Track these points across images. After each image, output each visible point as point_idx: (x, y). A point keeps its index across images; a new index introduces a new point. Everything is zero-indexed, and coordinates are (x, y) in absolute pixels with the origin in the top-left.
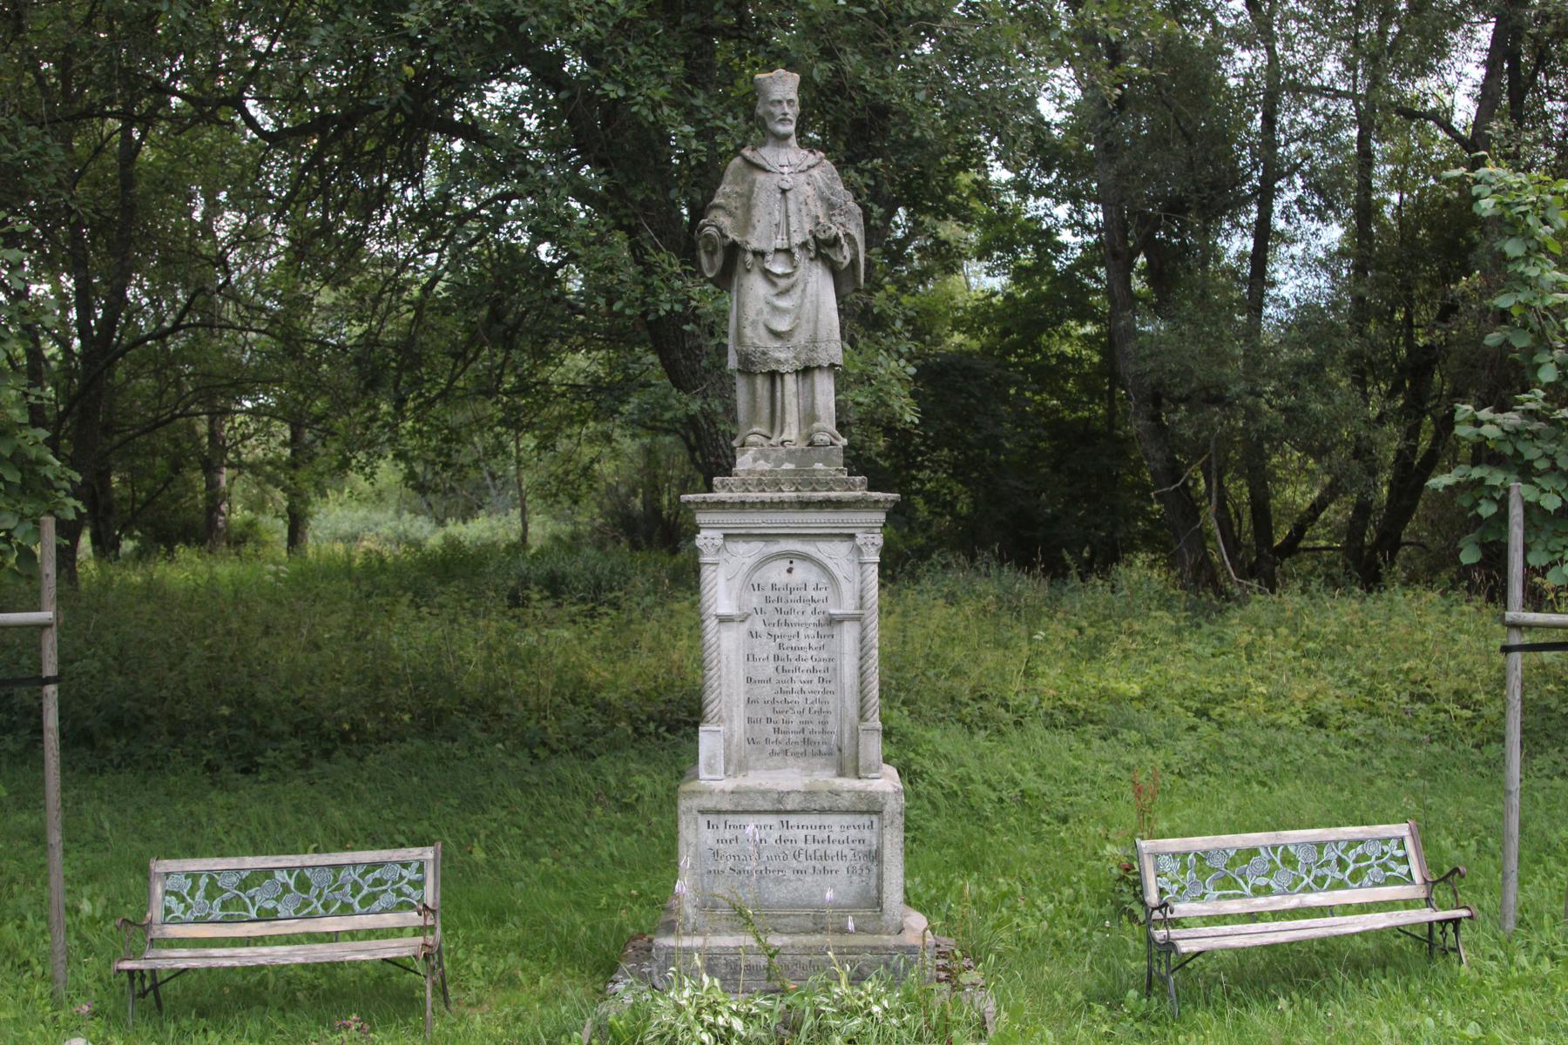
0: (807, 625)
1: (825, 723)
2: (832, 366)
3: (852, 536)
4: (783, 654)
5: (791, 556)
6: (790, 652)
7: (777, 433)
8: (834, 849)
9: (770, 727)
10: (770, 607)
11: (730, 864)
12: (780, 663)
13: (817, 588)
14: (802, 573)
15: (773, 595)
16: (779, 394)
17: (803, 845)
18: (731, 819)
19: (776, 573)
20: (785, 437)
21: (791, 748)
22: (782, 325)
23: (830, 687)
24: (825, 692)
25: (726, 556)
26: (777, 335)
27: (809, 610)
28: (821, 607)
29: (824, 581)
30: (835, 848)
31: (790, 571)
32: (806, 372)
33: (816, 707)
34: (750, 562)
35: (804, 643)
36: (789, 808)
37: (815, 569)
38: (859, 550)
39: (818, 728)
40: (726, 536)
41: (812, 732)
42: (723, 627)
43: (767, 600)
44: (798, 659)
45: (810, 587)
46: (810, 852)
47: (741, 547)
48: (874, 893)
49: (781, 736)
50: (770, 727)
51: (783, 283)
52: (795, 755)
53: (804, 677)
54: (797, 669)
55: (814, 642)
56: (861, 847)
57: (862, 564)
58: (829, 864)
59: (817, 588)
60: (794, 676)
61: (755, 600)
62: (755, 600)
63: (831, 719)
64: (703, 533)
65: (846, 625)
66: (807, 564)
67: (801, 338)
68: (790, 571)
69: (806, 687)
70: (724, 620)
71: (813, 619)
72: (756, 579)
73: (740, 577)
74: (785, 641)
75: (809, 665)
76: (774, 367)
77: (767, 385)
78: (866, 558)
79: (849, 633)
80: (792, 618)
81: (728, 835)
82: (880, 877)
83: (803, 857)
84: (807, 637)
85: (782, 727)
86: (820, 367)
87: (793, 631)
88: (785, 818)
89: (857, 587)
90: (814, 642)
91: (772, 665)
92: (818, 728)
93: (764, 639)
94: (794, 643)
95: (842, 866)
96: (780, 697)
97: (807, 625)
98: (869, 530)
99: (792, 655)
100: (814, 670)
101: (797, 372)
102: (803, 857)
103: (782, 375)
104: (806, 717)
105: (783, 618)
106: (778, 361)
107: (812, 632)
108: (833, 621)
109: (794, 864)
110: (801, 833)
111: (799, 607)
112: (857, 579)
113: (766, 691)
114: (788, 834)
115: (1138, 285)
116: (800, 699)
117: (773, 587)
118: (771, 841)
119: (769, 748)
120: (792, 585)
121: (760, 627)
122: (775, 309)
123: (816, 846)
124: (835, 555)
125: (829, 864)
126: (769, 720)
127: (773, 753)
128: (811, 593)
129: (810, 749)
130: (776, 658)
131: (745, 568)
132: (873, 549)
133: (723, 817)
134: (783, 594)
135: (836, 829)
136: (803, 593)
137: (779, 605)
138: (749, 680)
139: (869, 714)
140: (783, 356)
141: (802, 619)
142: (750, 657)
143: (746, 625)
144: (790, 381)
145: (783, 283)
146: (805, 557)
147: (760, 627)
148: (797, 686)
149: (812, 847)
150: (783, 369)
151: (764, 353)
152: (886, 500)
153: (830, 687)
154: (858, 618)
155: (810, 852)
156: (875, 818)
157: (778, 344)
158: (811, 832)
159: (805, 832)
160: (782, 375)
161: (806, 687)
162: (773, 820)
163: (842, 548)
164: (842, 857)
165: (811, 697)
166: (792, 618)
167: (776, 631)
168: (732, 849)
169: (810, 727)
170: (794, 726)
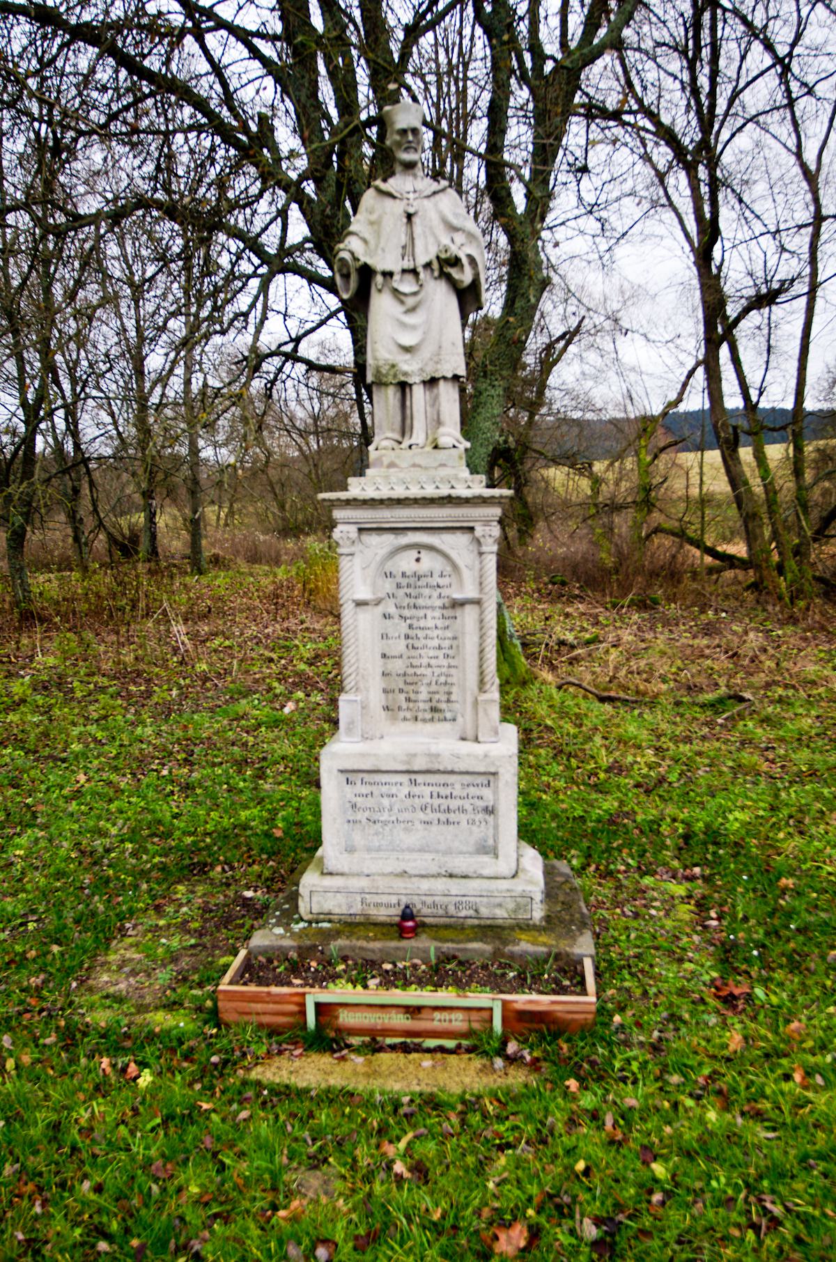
0: (433, 608)
1: (449, 693)
2: (456, 378)
3: (472, 529)
4: (412, 633)
5: (419, 547)
7: (407, 437)
8: (454, 804)
9: (402, 697)
10: (401, 592)
11: (367, 814)
12: (410, 641)
14: (429, 562)
15: (404, 582)
16: (408, 403)
17: (429, 800)
18: (367, 777)
19: (406, 562)
20: (413, 441)
21: (420, 715)
22: (408, 340)
23: (453, 662)
24: (449, 667)
25: (360, 547)
26: (407, 349)
27: (435, 594)
28: (445, 592)
29: (449, 569)
30: (454, 804)
31: (418, 560)
32: (432, 382)
33: (442, 679)
34: (383, 552)
35: (430, 623)
36: (416, 768)
37: (440, 559)
38: (479, 543)
39: (444, 698)
40: (360, 530)
41: (438, 701)
42: (359, 609)
43: (399, 586)
45: (436, 575)
46: (435, 806)
47: (373, 539)
48: (491, 842)
49: (411, 705)
50: (402, 697)
51: (410, 301)
52: (424, 720)
53: (432, 653)
54: (425, 647)
55: (439, 625)
56: (481, 804)
57: (481, 554)
58: (452, 817)
60: (422, 652)
61: (389, 586)
62: (389, 586)
63: (454, 689)
64: (340, 528)
65: (468, 608)
66: (434, 554)
67: (426, 353)
68: (418, 560)
69: (433, 662)
70: (360, 604)
71: (439, 603)
72: (389, 567)
73: (373, 566)
74: (416, 624)
75: (436, 643)
76: (403, 379)
77: (399, 395)
78: (484, 549)
79: (469, 616)
80: (420, 602)
81: (365, 790)
82: (496, 827)
83: (429, 810)
84: (433, 619)
85: (413, 696)
86: (444, 378)
87: (421, 613)
88: (413, 777)
89: (477, 574)
90: (440, 623)
91: (403, 642)
92: (444, 698)
93: (397, 620)
94: (422, 623)
95: (463, 818)
97: (433, 608)
98: (487, 523)
99: (421, 634)
100: (440, 648)
101: (424, 382)
102: (429, 810)
103: (411, 385)
104: (434, 688)
105: (412, 601)
106: (405, 374)
107: (438, 613)
108: (457, 604)
109: (422, 816)
110: (427, 791)
111: (426, 592)
112: (477, 566)
113: (398, 666)
114: (416, 790)
116: (428, 671)
117: (404, 575)
118: (402, 795)
119: (402, 714)
120: (421, 573)
121: (392, 610)
122: (403, 325)
123: (441, 801)
124: (456, 544)
125: (452, 817)
126: (401, 691)
127: (405, 719)
128: (436, 580)
129: (436, 715)
130: (407, 637)
131: (378, 558)
132: (491, 541)
133: (361, 775)
134: (412, 580)
135: (458, 786)
136: (429, 580)
137: (408, 591)
138: (384, 656)
139: (488, 686)
140: (412, 368)
141: (429, 603)
142: (384, 636)
143: (380, 609)
144: (419, 393)
145: (410, 301)
146: (431, 548)
147: (392, 610)
148: (425, 661)
149: (436, 802)
150: (410, 381)
151: (393, 366)
152: (501, 497)
153: (453, 662)
154: (478, 602)
155: (435, 806)
156: (491, 778)
157: (408, 356)
158: (435, 789)
159: (431, 788)
160: (411, 385)
161: (433, 662)
162: (404, 778)
163: (463, 539)
164: (462, 810)
165: (437, 671)
167: (406, 613)
168: (370, 802)
169: (437, 697)
170: (424, 695)
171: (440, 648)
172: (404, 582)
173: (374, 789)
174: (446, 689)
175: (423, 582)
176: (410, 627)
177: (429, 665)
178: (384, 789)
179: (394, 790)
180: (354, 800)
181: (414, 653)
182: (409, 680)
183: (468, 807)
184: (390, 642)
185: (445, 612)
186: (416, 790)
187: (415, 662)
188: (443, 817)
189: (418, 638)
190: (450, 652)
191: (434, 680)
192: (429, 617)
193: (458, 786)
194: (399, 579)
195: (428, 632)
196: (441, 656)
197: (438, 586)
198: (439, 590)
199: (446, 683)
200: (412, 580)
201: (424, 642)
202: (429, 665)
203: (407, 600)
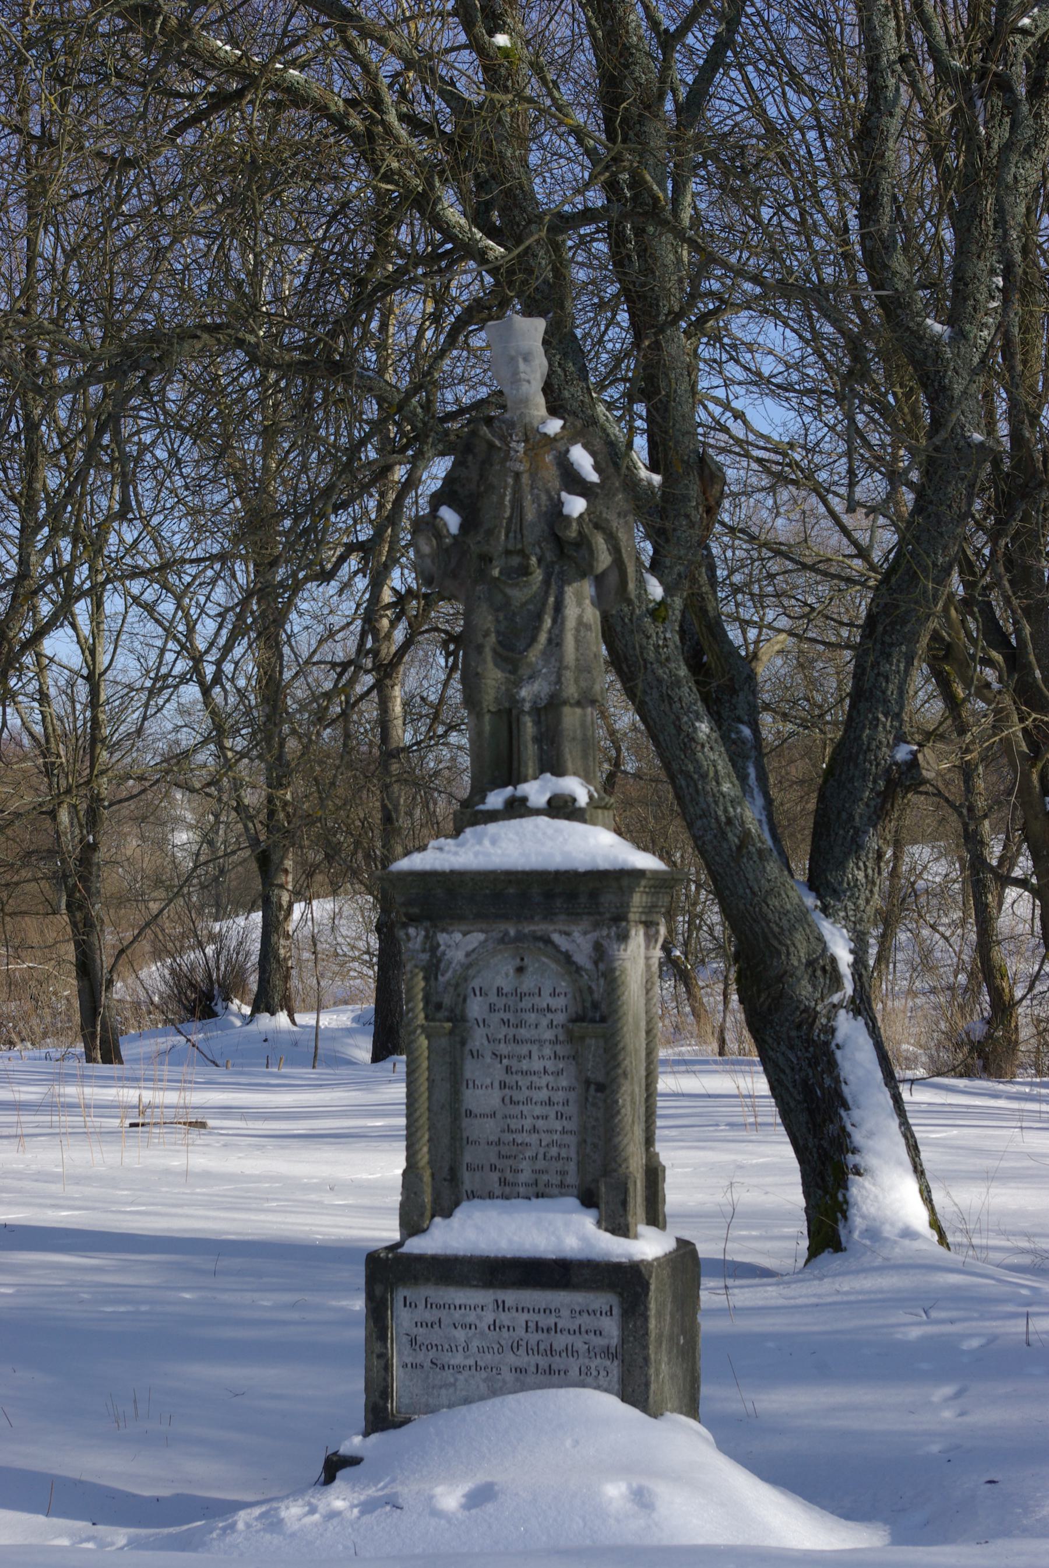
0: (541, 1042)
4: (511, 1080)
6: (519, 1078)
8: (560, 1341)
9: (495, 1176)
10: (496, 1018)
13: (554, 994)
15: (500, 1002)
24: (564, 1132)
27: (545, 1022)
30: (560, 1341)
33: (554, 1151)
35: (537, 1065)
43: (492, 1008)
44: (530, 1087)
45: (546, 992)
46: (533, 1343)
49: (507, 1189)
50: (495, 1176)
53: (538, 1110)
54: (529, 1100)
55: (551, 1068)
58: (558, 1362)
59: (554, 994)
60: (525, 1109)
69: (540, 1123)
71: (548, 1035)
74: (514, 1063)
75: (544, 1094)
80: (523, 1032)
81: (429, 1316)
83: (522, 1350)
85: (509, 1176)
87: (524, 1050)
90: (550, 1065)
93: (488, 1060)
94: (525, 1065)
96: (509, 1137)
100: (550, 1102)
102: (522, 1350)
104: (541, 1164)
105: (511, 1032)
107: (547, 1051)
109: (511, 1359)
111: (532, 1017)
114: (504, 1318)
115: (669, 106)
116: (534, 1138)
117: (499, 991)
118: (483, 1326)
123: (540, 1336)
125: (558, 1362)
126: (493, 1168)
130: (503, 1085)
134: (511, 1001)
135: (565, 1313)
136: (536, 1000)
137: (506, 1016)
141: (532, 1033)
148: (528, 1123)
149: (533, 1338)
155: (533, 1343)
158: (534, 1317)
161: (540, 1123)
164: (571, 1351)
165: (546, 1139)
166: (523, 1032)
167: (503, 1049)
169: (545, 1177)
171: (550, 1102)
172: (500, 1002)
173: (443, 1314)
174: (558, 1165)
175: (527, 1003)
176: (508, 1070)
177: (534, 1130)
178: (457, 1315)
179: (472, 1317)
180: (415, 1331)
181: (515, 1110)
182: (505, 1150)
183: (580, 1346)
184: (479, 1092)
185: (558, 1048)
186: (504, 1318)
187: (514, 1124)
188: (543, 1362)
189: (518, 1087)
190: (566, 1110)
191: (542, 1151)
192: (535, 1056)
193: (565, 1313)
194: (493, 998)
195: (535, 1078)
196: (553, 1115)
197: (549, 1010)
198: (550, 1016)
199: (558, 1157)
200: (511, 1001)
201: (527, 1093)
202: (534, 1130)
203: (504, 1030)
